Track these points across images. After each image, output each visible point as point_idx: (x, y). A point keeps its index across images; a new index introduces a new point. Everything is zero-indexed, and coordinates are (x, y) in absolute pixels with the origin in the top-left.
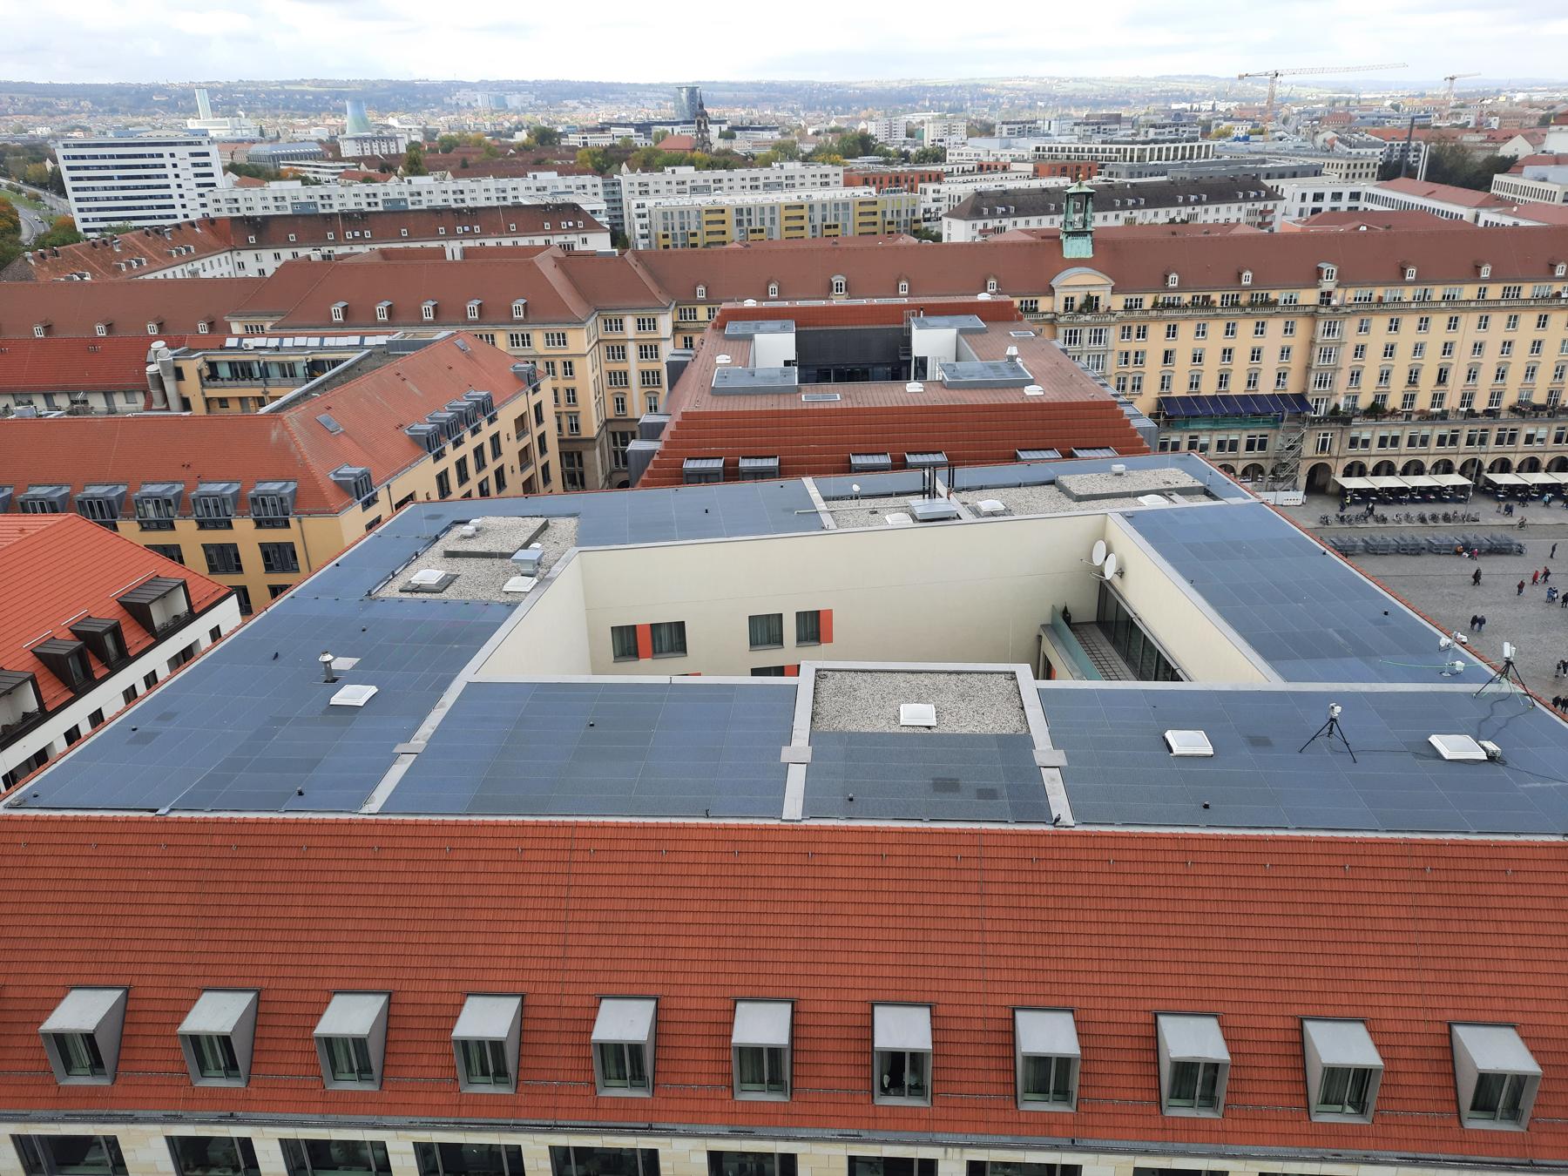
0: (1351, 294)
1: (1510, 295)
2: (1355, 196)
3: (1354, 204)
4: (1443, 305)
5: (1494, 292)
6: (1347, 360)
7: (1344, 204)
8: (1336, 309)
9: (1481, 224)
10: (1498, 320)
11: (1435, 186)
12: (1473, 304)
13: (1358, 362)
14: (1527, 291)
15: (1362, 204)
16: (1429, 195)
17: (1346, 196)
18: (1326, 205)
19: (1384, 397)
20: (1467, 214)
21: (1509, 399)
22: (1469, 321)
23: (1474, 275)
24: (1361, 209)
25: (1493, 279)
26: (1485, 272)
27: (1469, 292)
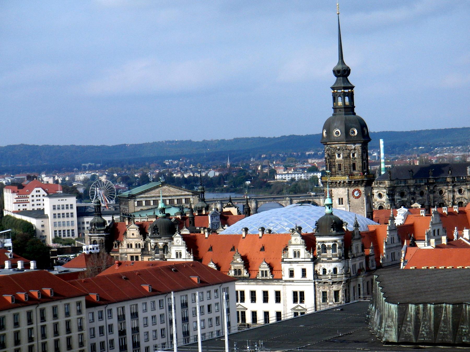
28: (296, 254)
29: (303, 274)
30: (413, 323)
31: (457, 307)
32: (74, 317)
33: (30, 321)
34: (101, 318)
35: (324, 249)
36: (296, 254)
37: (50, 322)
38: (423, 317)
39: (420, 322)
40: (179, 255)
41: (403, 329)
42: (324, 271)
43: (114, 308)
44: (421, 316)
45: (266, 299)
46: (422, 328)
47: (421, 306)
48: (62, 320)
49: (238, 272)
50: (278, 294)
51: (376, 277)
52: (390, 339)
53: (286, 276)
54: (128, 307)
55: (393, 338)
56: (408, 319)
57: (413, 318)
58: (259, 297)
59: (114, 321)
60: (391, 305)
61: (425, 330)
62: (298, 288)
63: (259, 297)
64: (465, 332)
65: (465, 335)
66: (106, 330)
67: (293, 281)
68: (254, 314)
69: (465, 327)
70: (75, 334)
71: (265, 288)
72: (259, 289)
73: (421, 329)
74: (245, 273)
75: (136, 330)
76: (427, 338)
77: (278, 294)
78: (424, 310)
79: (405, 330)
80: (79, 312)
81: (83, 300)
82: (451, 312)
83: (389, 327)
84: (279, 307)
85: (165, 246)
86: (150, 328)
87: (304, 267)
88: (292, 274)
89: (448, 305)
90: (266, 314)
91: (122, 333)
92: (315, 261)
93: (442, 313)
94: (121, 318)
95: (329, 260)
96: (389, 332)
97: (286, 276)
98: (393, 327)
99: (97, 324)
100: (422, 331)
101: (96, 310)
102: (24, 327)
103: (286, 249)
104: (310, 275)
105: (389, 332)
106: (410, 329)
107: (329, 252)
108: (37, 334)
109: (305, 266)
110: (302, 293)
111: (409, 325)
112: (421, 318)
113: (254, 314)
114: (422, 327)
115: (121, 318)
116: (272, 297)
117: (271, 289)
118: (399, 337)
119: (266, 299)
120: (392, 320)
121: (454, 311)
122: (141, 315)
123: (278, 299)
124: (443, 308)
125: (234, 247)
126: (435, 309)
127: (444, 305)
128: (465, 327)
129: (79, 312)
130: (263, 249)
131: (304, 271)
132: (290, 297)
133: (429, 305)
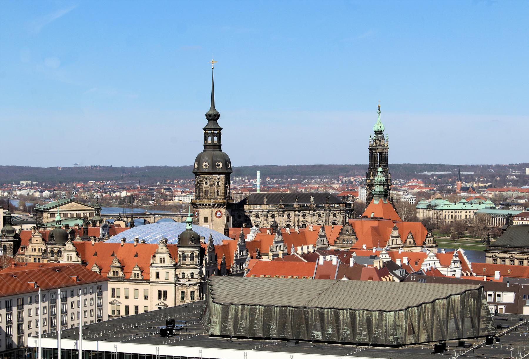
28: (162, 260)
29: (157, 276)
30: (233, 320)
31: (268, 309)
35: (184, 257)
36: (162, 260)
38: (241, 316)
39: (238, 320)
41: (225, 324)
42: (184, 274)
44: (239, 315)
46: (240, 324)
47: (240, 307)
51: (210, 281)
52: (215, 332)
56: (229, 317)
57: (233, 317)
60: (217, 305)
61: (242, 327)
62: (162, 288)
64: (273, 328)
65: (272, 330)
67: (158, 283)
68: (127, 307)
69: (273, 324)
73: (239, 325)
74: (121, 275)
76: (243, 333)
78: (242, 310)
79: (227, 326)
82: (263, 313)
83: (214, 322)
87: (158, 271)
89: (261, 307)
90: (137, 308)
93: (256, 313)
96: (214, 327)
97: (153, 278)
98: (217, 323)
100: (239, 327)
103: (154, 256)
105: (214, 327)
107: (188, 260)
109: (169, 270)
110: (165, 292)
111: (230, 322)
112: (240, 317)
113: (127, 307)
114: (240, 323)
117: (141, 287)
118: (221, 331)
120: (217, 317)
121: (265, 311)
124: (257, 308)
125: (96, 252)
126: (251, 309)
127: (258, 307)
128: (273, 324)
130: (136, 256)
133: (246, 306)
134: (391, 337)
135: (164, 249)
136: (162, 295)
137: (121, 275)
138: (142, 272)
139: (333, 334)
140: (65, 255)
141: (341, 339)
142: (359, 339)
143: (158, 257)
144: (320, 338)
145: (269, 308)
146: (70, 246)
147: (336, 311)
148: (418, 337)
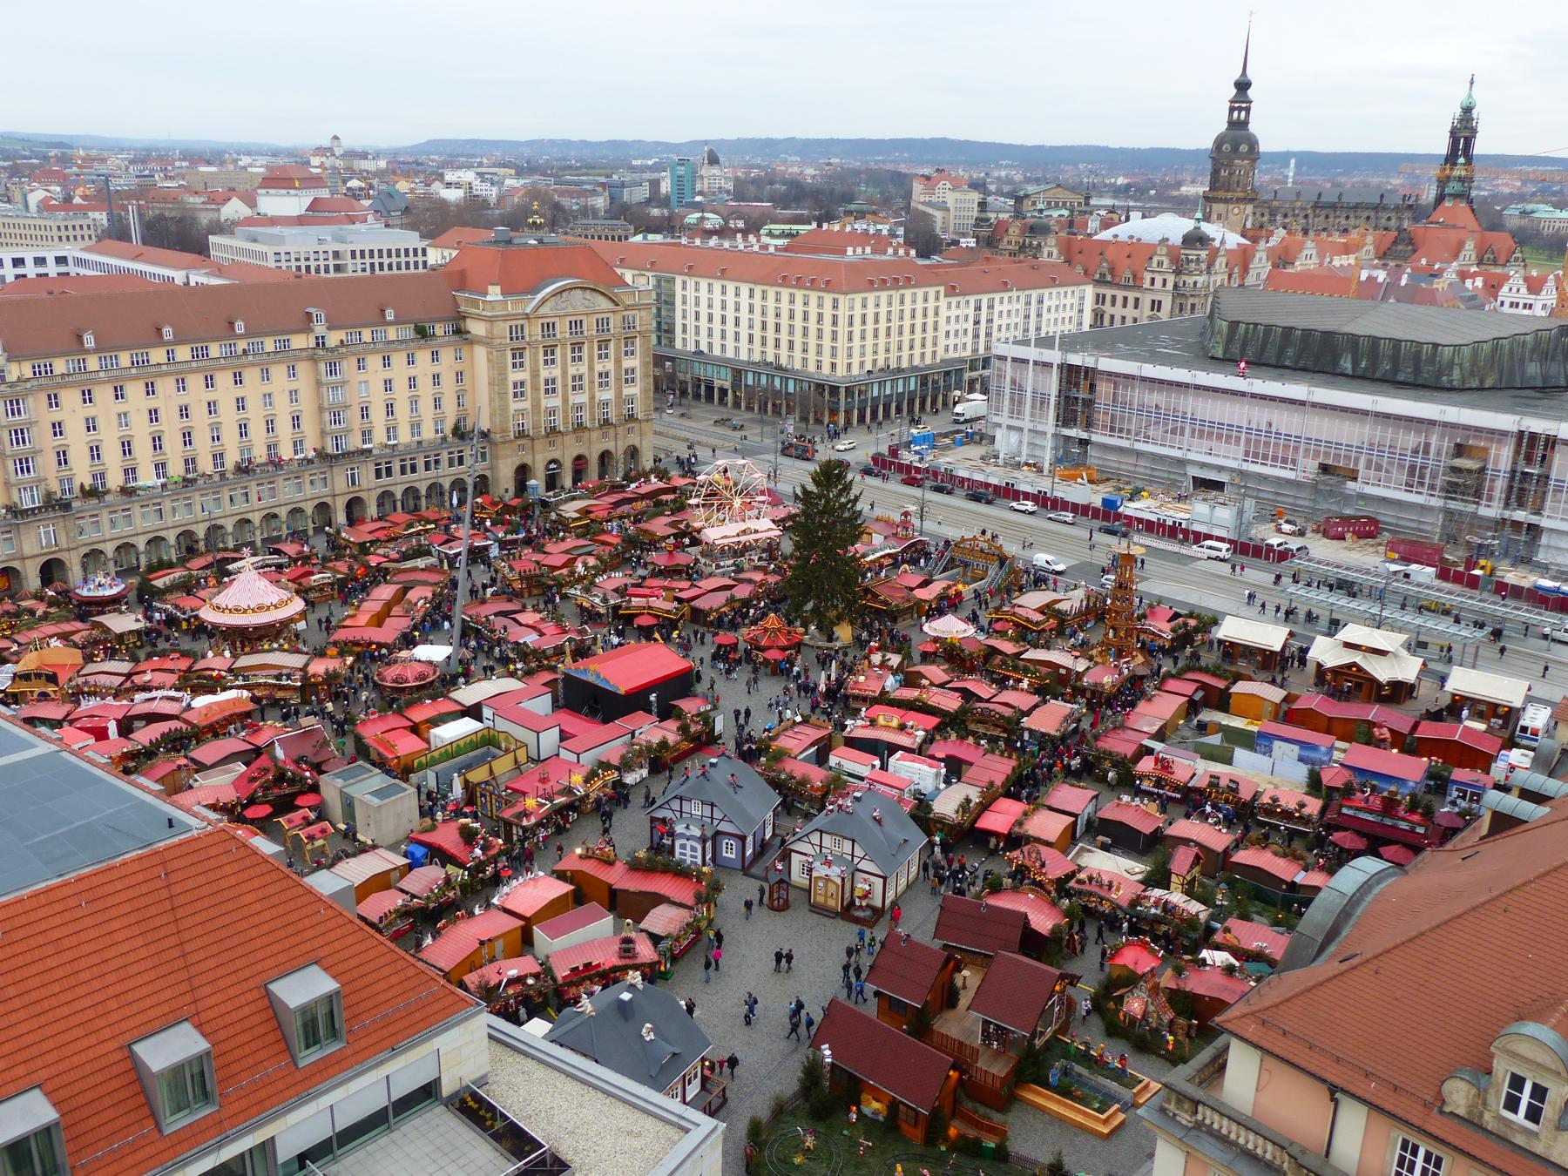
0: (27, 370)
1: (200, 354)
2: (61, 260)
3: (63, 269)
4: (134, 371)
5: (183, 353)
6: (42, 438)
7: (52, 269)
8: (12, 385)
9: (192, 283)
10: (195, 382)
11: (150, 250)
12: (164, 368)
13: (59, 440)
14: (215, 350)
15: (72, 269)
16: (137, 257)
17: (51, 261)
18: (31, 270)
19: (102, 475)
20: (179, 277)
21: (231, 459)
22: (165, 386)
23: (158, 340)
24: (73, 274)
25: (178, 341)
26: (168, 333)
27: (158, 355)
28: (1160, 264)
32: (931, 304)
33: (890, 304)
34: (958, 306)
35: (1189, 261)
36: (1160, 264)
37: (908, 307)
40: (1050, 254)
43: (972, 299)
45: (1125, 306)
48: (920, 306)
49: (1103, 275)
50: (1137, 300)
53: (1147, 285)
54: (985, 299)
55: (1219, 353)
58: (1119, 301)
59: (971, 311)
62: (1157, 298)
63: (1119, 301)
66: (961, 319)
68: (1112, 317)
70: (930, 320)
71: (1126, 293)
72: (1120, 294)
74: (1109, 278)
75: (990, 321)
77: (1137, 300)
80: (937, 299)
81: (942, 289)
84: (1136, 313)
85: (1039, 245)
86: (1004, 321)
88: (1153, 280)
90: (1124, 318)
91: (977, 323)
92: (1178, 272)
94: (978, 308)
95: (1190, 274)
97: (1147, 285)
99: (954, 312)
101: (954, 300)
102: (883, 310)
104: (1170, 286)
106: (1236, 349)
107: (1193, 265)
108: (895, 316)
113: (1112, 317)
115: (978, 308)
116: (1131, 303)
117: (1131, 295)
118: (1226, 350)
119: (1125, 306)
122: (997, 307)
123: (1136, 307)
129: (937, 299)
131: (1164, 284)
132: (1148, 304)
134: (1444, 379)
135: (1164, 251)
136: (1156, 305)
137: (1109, 278)
138: (1135, 277)
139: (1366, 369)
140: (1046, 251)
141: (1378, 375)
142: (1401, 377)
143: (1155, 260)
144: (1349, 371)
145: (1288, 330)
146: (1052, 240)
147: (1374, 341)
148: (1482, 381)
